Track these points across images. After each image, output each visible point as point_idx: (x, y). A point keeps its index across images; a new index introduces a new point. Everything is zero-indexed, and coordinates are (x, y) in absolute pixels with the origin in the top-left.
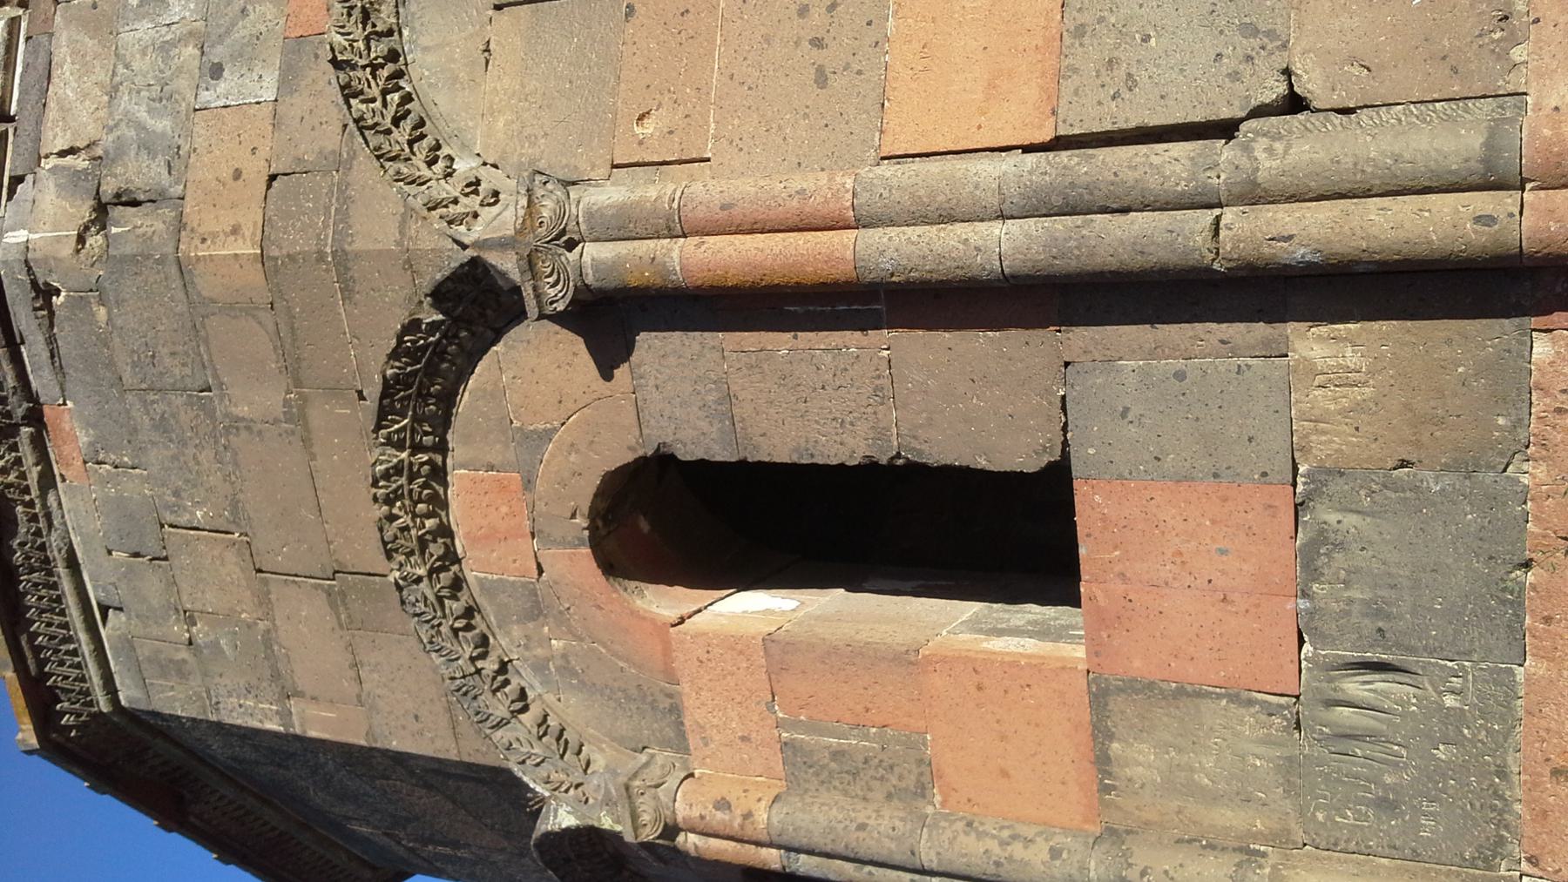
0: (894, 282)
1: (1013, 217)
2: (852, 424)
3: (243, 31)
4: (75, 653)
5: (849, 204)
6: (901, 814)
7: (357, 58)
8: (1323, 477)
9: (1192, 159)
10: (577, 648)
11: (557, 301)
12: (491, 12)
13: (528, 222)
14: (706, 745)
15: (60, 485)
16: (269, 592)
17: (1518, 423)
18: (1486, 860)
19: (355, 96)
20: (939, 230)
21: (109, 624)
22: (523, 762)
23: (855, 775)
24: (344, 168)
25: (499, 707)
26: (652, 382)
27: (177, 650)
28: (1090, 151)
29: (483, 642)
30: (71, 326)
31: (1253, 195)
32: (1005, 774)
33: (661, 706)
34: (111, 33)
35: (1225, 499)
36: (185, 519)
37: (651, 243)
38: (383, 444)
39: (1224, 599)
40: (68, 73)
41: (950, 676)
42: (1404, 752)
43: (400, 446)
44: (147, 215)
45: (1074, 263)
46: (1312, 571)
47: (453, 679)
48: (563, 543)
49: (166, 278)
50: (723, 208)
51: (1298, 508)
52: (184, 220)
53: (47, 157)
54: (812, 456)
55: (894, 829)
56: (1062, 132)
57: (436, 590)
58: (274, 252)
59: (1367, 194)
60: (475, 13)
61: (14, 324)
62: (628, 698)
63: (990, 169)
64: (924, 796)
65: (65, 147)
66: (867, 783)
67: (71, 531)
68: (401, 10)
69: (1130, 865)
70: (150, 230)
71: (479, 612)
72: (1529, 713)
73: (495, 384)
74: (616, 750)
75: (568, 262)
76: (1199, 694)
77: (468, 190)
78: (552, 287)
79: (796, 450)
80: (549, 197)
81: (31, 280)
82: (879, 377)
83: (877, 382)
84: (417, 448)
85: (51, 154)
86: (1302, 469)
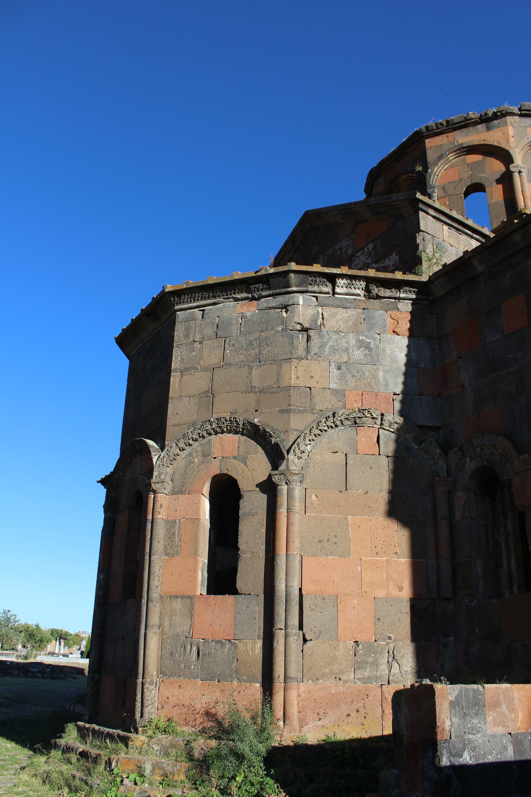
1: (286, 588)
2: (247, 546)
3: (349, 376)
4: (191, 301)
6: (162, 551)
8: (235, 645)
9: (294, 625)
12: (345, 453)
13: (292, 474)
14: (174, 500)
16: (208, 372)
17: (244, 680)
18: (162, 672)
19: (326, 419)
21: (199, 312)
22: (168, 451)
24: (311, 411)
25: (181, 445)
27: (192, 336)
29: (196, 440)
30: (277, 317)
31: (286, 636)
32: (172, 574)
33: (183, 488)
34: (353, 330)
35: (231, 626)
37: (286, 504)
38: (244, 421)
40: (344, 315)
42: (182, 658)
44: (304, 347)
46: (217, 642)
47: (187, 433)
48: (220, 466)
49: (287, 354)
50: (292, 523)
51: (229, 640)
52: (301, 360)
53: (322, 309)
54: (240, 535)
56: (304, 596)
59: (285, 657)
62: (184, 479)
63: (296, 584)
64: (166, 555)
65: (324, 316)
68: (349, 426)
69: (156, 603)
70: (299, 349)
72: (191, 681)
74: (171, 474)
76: (191, 618)
77: (302, 452)
79: (241, 531)
84: (243, 429)
86: (236, 641)
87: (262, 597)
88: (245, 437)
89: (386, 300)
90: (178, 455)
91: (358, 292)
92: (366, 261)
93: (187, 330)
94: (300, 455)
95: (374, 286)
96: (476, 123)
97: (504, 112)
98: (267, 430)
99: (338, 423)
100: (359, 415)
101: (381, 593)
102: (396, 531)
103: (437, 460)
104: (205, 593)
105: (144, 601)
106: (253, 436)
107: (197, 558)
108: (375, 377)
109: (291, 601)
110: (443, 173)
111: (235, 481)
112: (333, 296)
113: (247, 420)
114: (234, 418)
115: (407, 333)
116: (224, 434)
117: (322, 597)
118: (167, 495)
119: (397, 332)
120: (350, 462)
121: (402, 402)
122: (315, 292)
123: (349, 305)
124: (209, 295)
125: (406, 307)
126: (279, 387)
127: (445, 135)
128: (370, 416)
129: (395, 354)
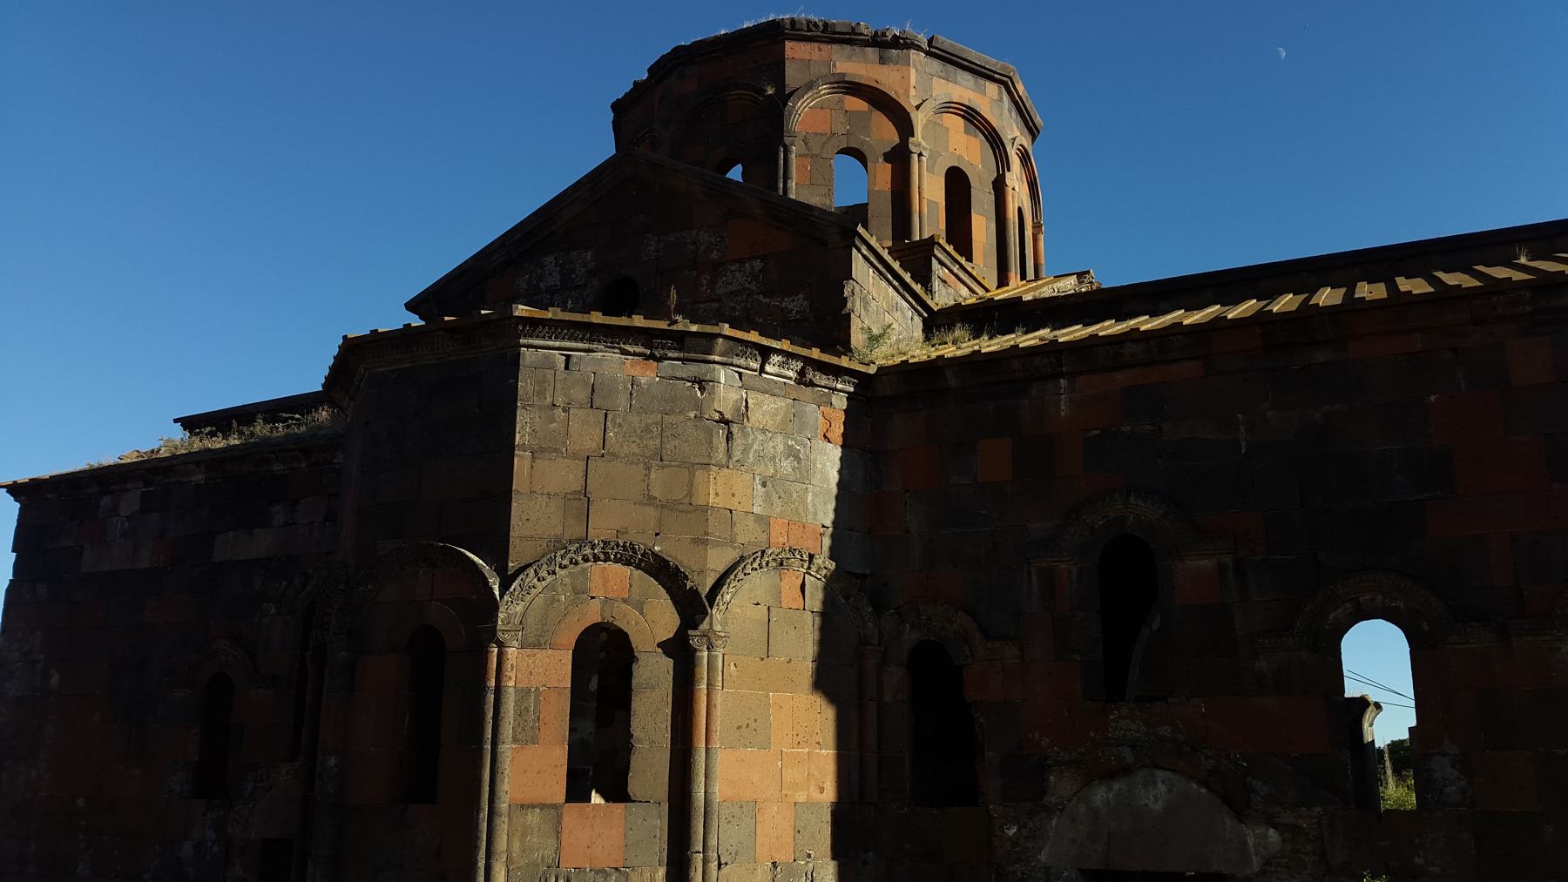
15: (623, 357)
21: (559, 356)
23: (520, 715)
51: (617, 869)
67: (603, 354)
70: (719, 451)
76: (558, 838)
87: (666, 806)
89: (820, 389)
91: (791, 374)
92: (747, 285)
95: (811, 369)
96: (866, 44)
97: (908, 41)
101: (801, 797)
105: (484, 814)
108: (803, 501)
110: (807, 112)
111: (626, 635)
114: (631, 544)
116: (608, 563)
120: (773, 619)
121: (833, 536)
122: (739, 367)
123: (777, 391)
124: (584, 336)
125: (840, 402)
127: (816, 45)
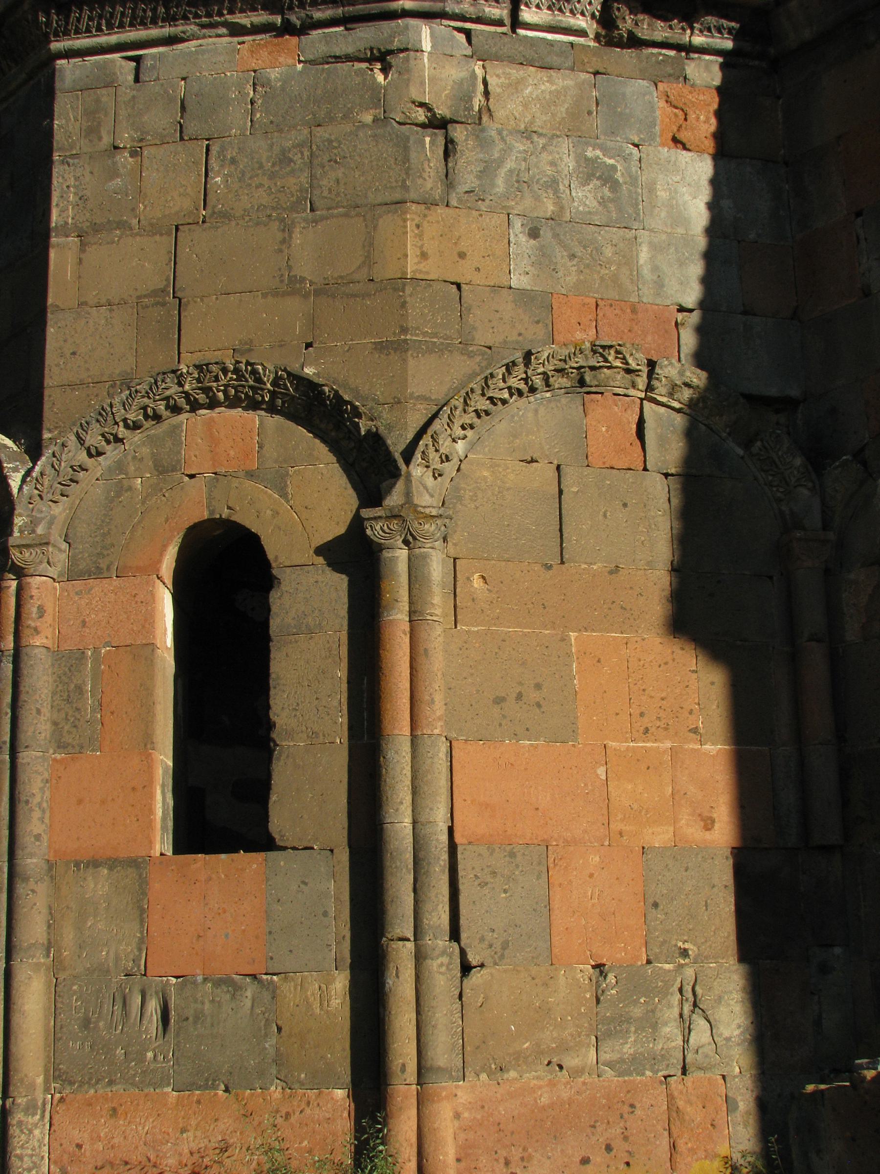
0: (379, 758)
1: (414, 829)
2: (295, 716)
3: (560, 255)
4: (99, 29)
5: (425, 732)
6: (48, 735)
7: (532, 368)
9: (439, 926)
10: (137, 499)
11: (372, 530)
12: (556, 462)
13: (421, 515)
14: (77, 593)
15: (236, 39)
16: (161, 235)
17: (302, 1084)
18: (60, 1076)
20: (408, 786)
21: (124, 63)
22: (54, 455)
23: (68, 701)
25: (94, 439)
26: (320, 579)
27: (109, 132)
28: (447, 870)
29: (136, 426)
30: (359, 84)
31: (419, 957)
32: (80, 802)
33: (100, 561)
34: (569, 130)
35: (257, 937)
36: (214, 165)
37: (406, 598)
38: (277, 373)
39: (199, 936)
40: (543, 87)
41: (140, 770)
42: (118, 1032)
43: (275, 383)
44: (437, 172)
45: (388, 864)
46: (218, 983)
47: (111, 406)
48: (210, 498)
49: (392, 188)
50: (426, 650)
51: (254, 976)
52: (433, 207)
53: (484, 67)
54: (275, 688)
55: (40, 733)
56: (459, 848)
57: (174, 396)
58: (408, 290)
59: (418, 1013)
60: (557, 450)
61: (361, 25)
62: (104, 535)
63: (440, 816)
64: (59, 747)
65: (490, 88)
66: (63, 709)
67: (200, 42)
69: (36, 883)
70: (426, 175)
71: (157, 423)
72: (146, 1095)
73: (318, 459)
75: (396, 541)
76: (142, 921)
78: (381, 527)
79: (278, 678)
80: (437, 528)
81: (394, 50)
82: (324, 736)
83: (321, 735)
84: (273, 394)
85: (486, 72)
86: (275, 977)
87: (343, 856)
88: (275, 421)
89: (655, 51)
90: (83, 470)
91: (581, 22)
93: (92, 113)
94: (439, 466)
95: (624, 9)
98: (346, 397)
99: (538, 381)
100: (593, 362)
102: (693, 671)
103: (795, 487)
104: (170, 853)
106: (303, 415)
107: (150, 754)
108: (628, 260)
109: (429, 864)
112: (514, 32)
113: (285, 370)
114: (248, 363)
115: (710, 145)
116: (218, 410)
117: (508, 848)
118: (54, 580)
119: (684, 141)
120: (571, 488)
121: (701, 330)
122: (463, 18)
123: (555, 60)
124: (154, 11)
126: (372, 280)
128: (620, 365)
129: (680, 202)
